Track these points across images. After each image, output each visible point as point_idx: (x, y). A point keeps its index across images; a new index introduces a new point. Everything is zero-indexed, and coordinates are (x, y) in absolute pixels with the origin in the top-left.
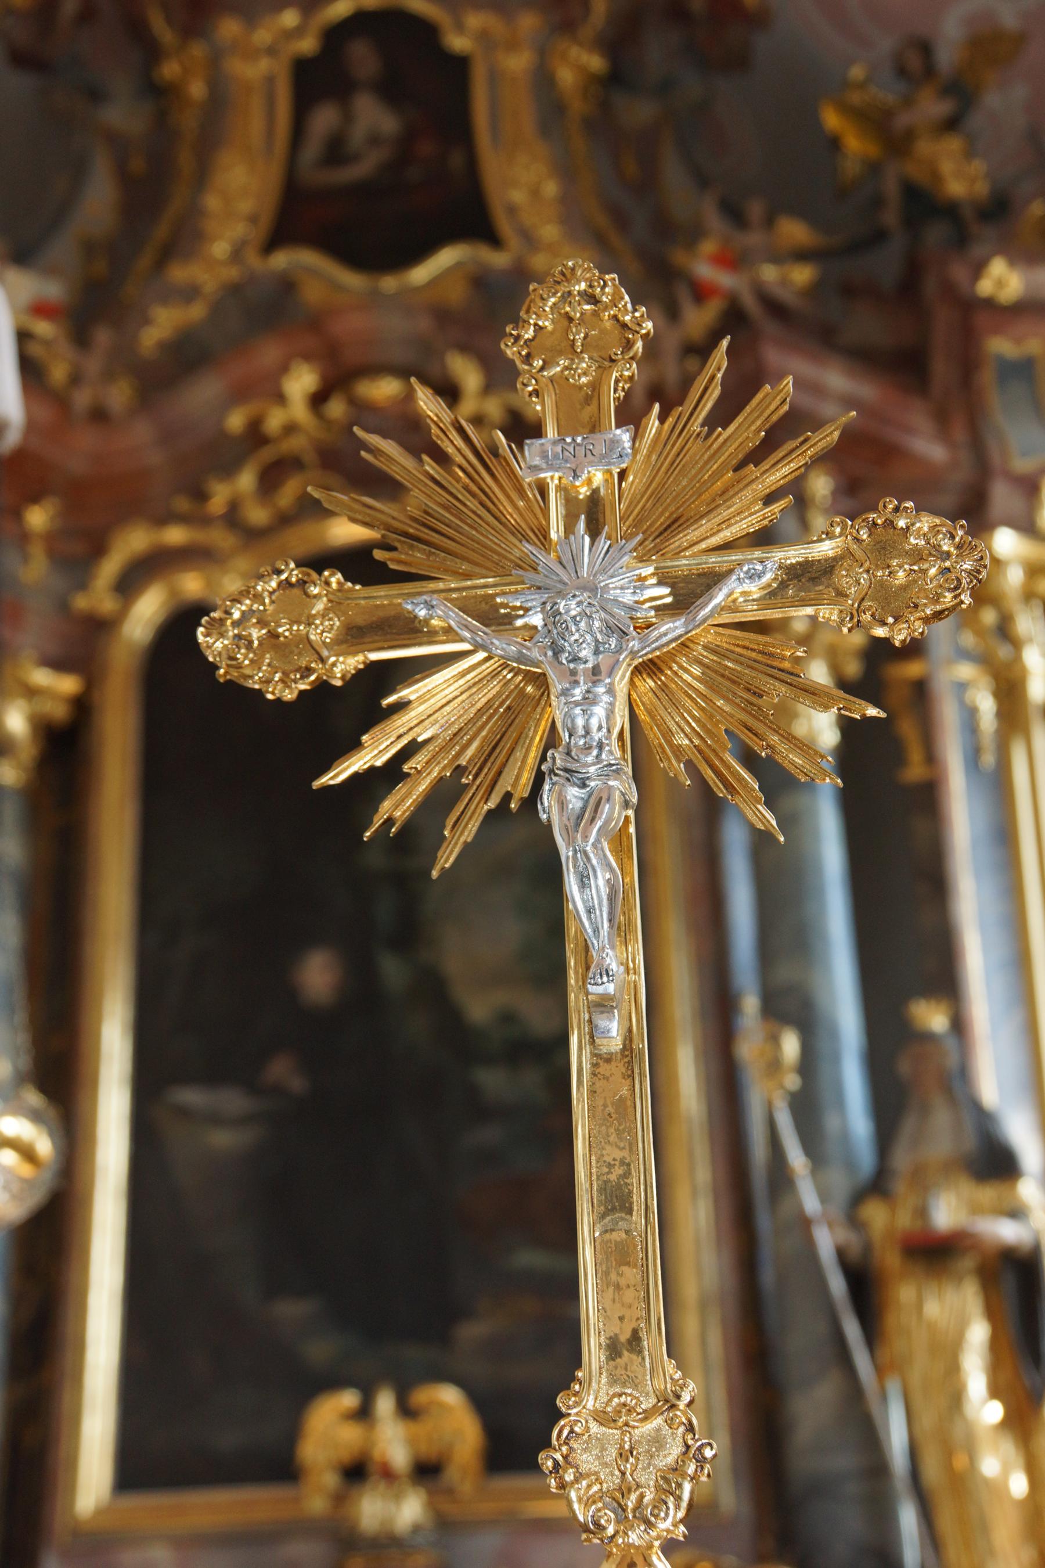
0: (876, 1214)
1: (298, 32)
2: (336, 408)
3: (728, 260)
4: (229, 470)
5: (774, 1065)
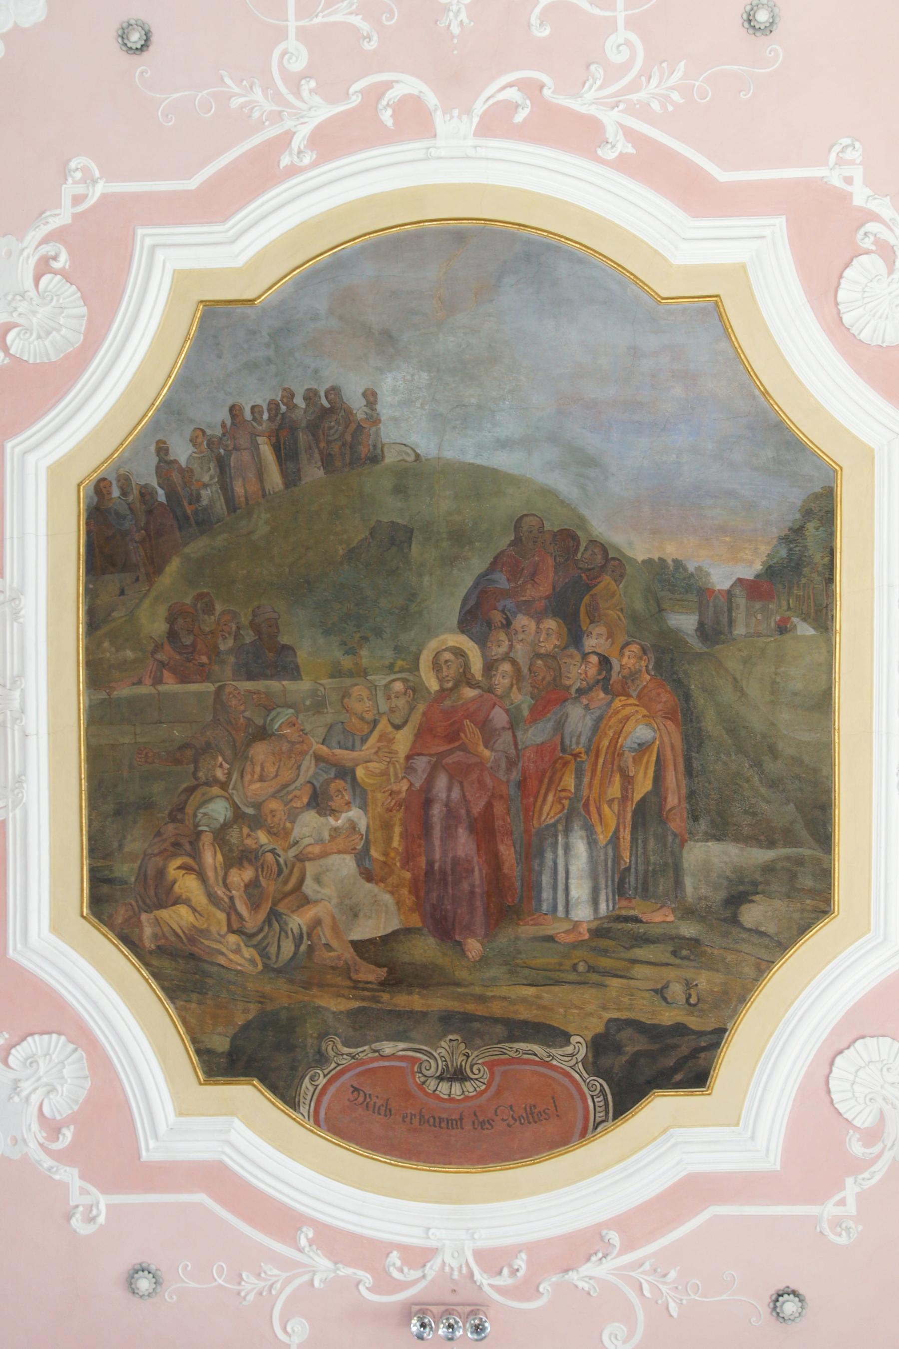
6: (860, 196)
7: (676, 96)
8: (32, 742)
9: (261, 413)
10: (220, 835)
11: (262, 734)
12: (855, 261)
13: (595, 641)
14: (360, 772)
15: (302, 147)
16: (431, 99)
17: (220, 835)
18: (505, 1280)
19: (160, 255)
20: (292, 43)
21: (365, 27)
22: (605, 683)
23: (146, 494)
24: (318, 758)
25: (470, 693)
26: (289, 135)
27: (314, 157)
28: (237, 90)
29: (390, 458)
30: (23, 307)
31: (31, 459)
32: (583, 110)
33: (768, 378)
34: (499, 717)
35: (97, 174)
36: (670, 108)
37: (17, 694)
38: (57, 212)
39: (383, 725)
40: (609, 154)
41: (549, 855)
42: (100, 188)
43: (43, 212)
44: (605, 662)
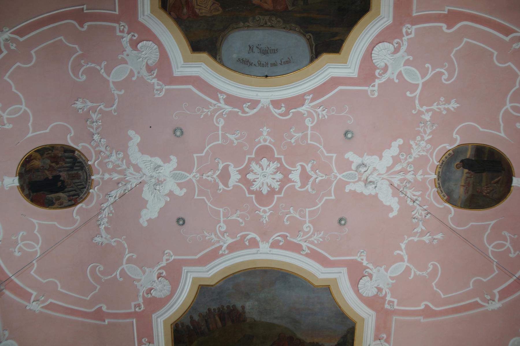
6: (365, 263)
7: (321, 240)
9: (216, 310)
12: (363, 278)
15: (225, 249)
16: (258, 239)
19: (189, 274)
20: (222, 224)
21: (241, 220)
23: (188, 327)
26: (221, 247)
27: (228, 252)
28: (207, 235)
29: (248, 321)
30: (155, 285)
31: (159, 320)
32: (298, 242)
33: (341, 303)
35: (172, 254)
36: (319, 242)
38: (162, 262)
40: (304, 253)
42: (173, 258)
43: (159, 263)
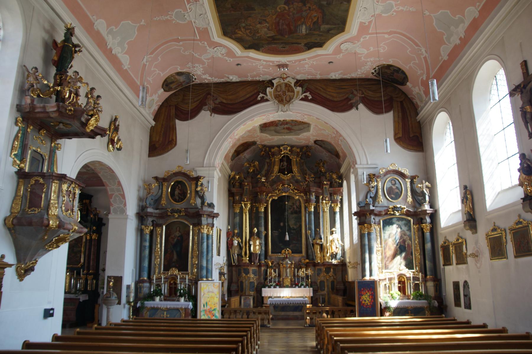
0: (314, 241)
1: (280, 157)
2: (283, 186)
3: (308, 178)
4: (276, 190)
5: (309, 233)
8: (210, 20)
10: (244, 27)
11: (250, 17)
13: (308, 5)
14: (267, 20)
17: (244, 27)
18: (291, 62)
22: (310, 10)
24: (260, 19)
25: (285, 11)
34: (291, 14)
37: (206, 16)
39: (271, 15)
41: (299, 28)
44: (310, 7)
